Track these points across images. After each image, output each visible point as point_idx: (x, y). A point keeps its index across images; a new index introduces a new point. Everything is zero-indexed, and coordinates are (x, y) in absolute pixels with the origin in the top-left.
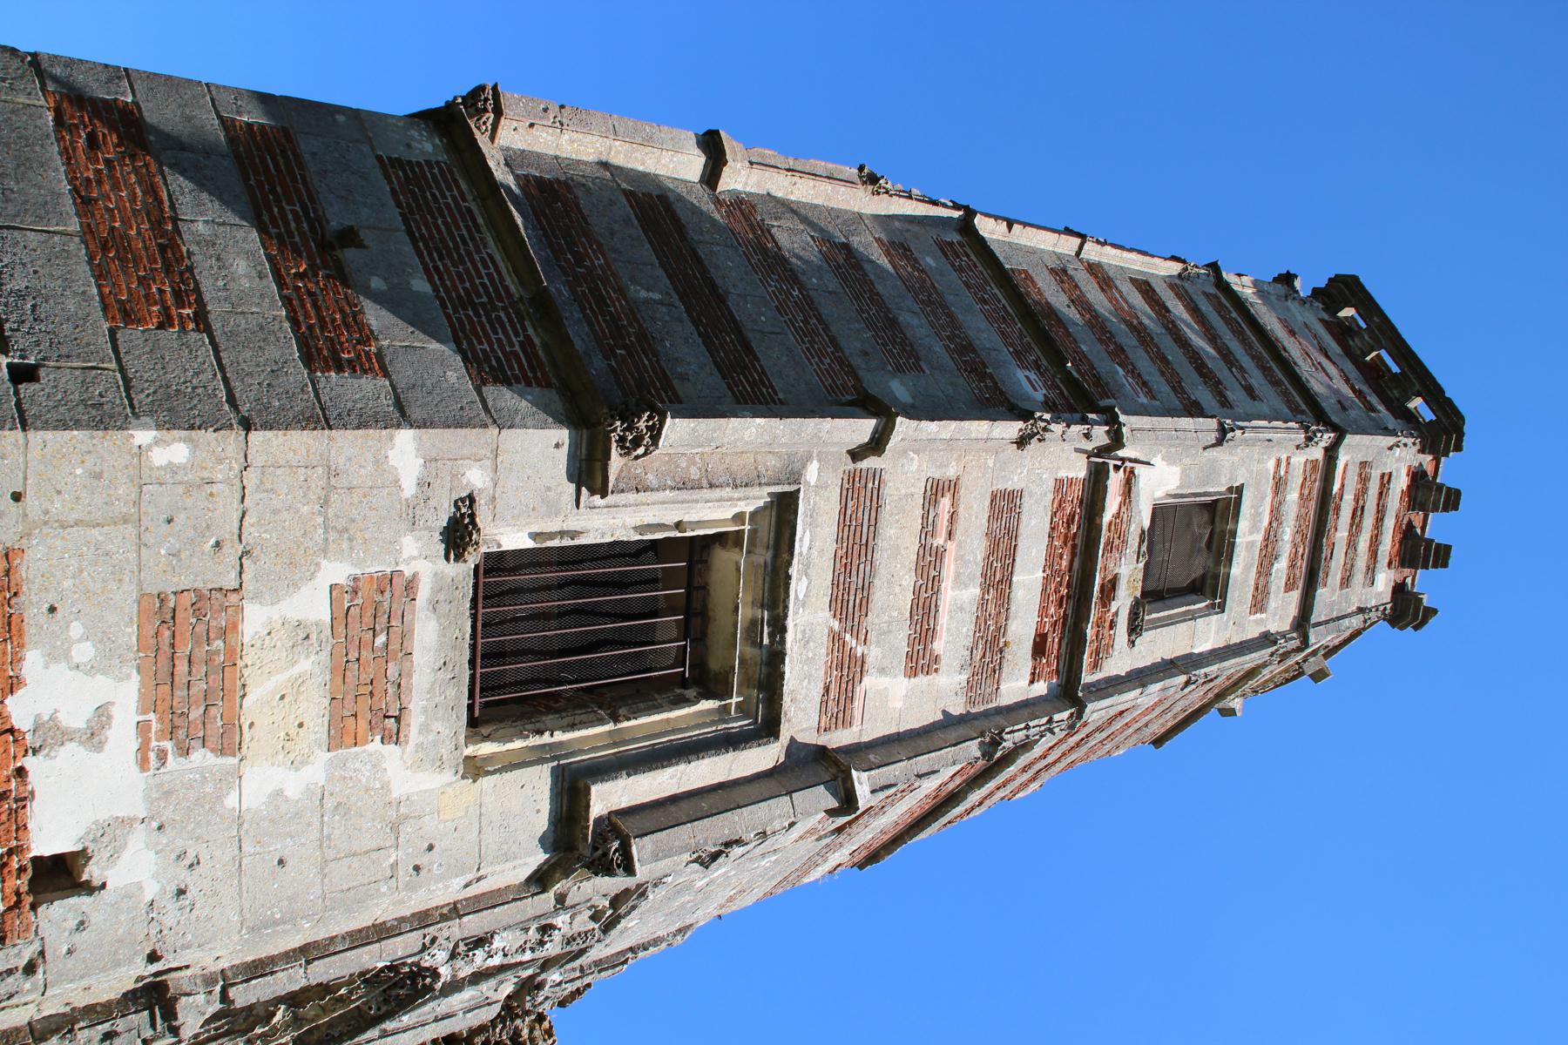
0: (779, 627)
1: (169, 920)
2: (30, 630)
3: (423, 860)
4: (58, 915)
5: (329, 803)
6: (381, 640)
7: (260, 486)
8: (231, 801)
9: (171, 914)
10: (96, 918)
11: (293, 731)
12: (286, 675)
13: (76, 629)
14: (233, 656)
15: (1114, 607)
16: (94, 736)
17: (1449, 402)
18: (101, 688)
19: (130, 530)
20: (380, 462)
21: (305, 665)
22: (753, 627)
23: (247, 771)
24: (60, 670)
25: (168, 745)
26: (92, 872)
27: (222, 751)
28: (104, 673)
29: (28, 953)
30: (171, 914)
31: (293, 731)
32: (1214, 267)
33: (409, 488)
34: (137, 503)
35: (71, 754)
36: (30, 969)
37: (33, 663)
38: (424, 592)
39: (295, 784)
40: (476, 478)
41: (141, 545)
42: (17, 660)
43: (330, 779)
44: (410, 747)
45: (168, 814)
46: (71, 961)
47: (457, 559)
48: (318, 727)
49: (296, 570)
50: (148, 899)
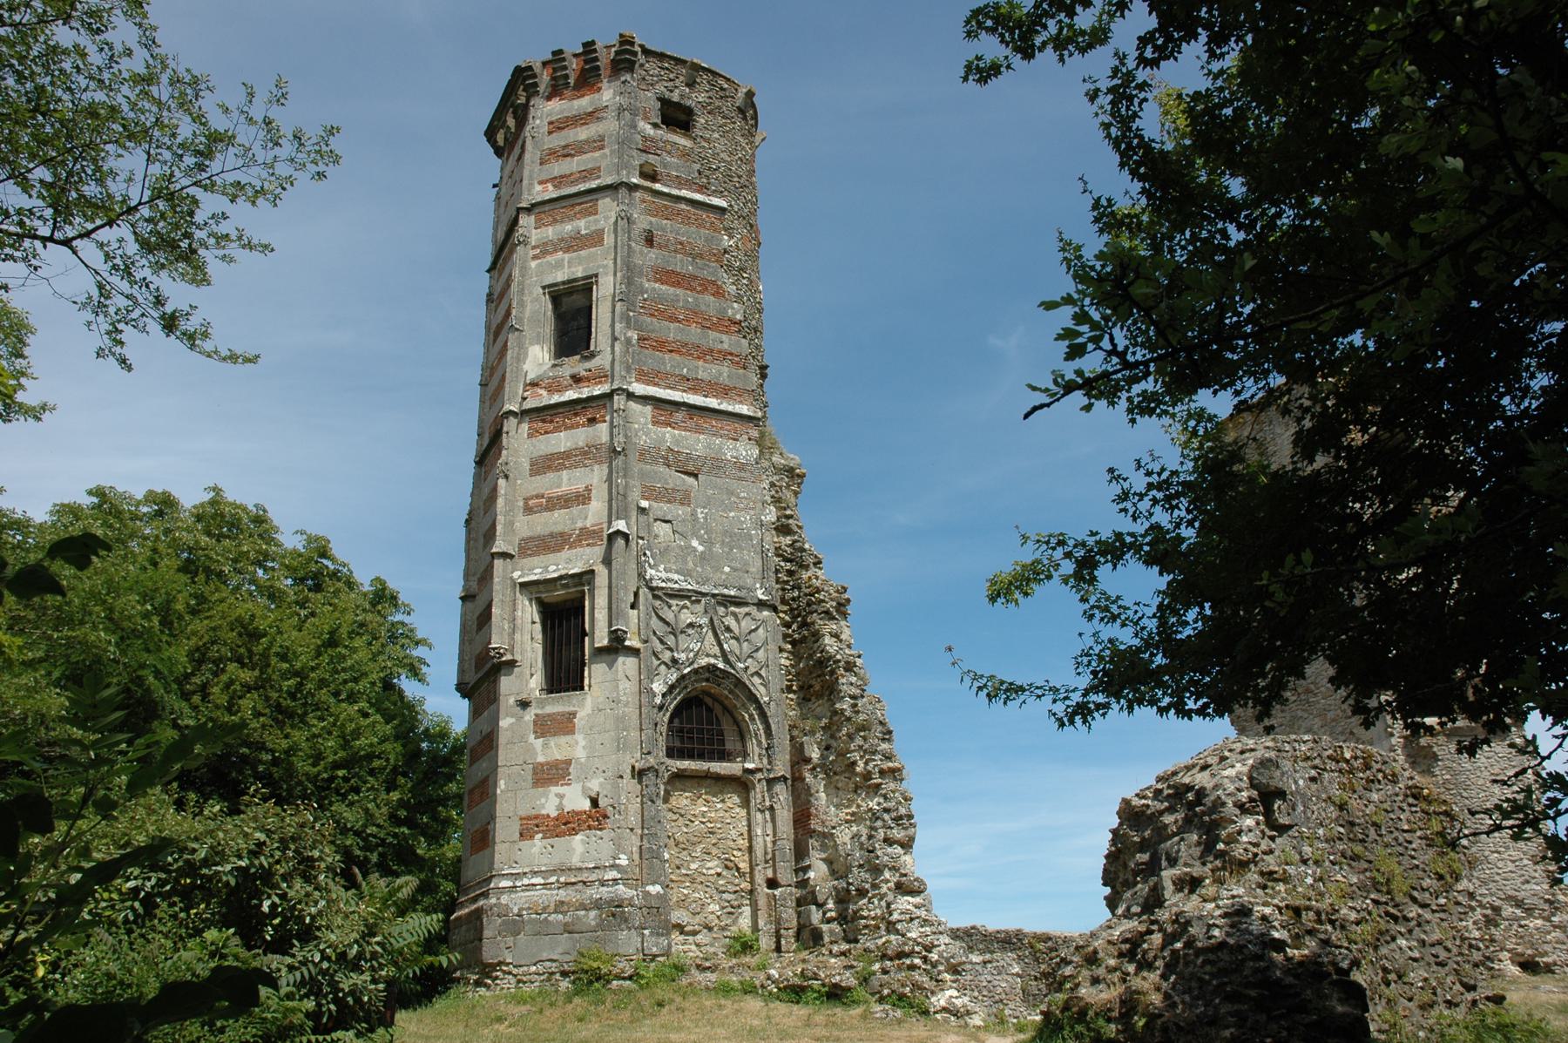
0: (561, 578)
4: (601, 803)
14: (548, 763)
15: (584, 373)
16: (561, 796)
17: (513, 75)
18: (551, 796)
21: (552, 744)
22: (565, 586)
26: (593, 795)
32: (488, 271)
33: (513, 720)
37: (544, 812)
38: (539, 712)
39: (582, 743)
40: (512, 700)
48: (568, 738)
49: (530, 750)
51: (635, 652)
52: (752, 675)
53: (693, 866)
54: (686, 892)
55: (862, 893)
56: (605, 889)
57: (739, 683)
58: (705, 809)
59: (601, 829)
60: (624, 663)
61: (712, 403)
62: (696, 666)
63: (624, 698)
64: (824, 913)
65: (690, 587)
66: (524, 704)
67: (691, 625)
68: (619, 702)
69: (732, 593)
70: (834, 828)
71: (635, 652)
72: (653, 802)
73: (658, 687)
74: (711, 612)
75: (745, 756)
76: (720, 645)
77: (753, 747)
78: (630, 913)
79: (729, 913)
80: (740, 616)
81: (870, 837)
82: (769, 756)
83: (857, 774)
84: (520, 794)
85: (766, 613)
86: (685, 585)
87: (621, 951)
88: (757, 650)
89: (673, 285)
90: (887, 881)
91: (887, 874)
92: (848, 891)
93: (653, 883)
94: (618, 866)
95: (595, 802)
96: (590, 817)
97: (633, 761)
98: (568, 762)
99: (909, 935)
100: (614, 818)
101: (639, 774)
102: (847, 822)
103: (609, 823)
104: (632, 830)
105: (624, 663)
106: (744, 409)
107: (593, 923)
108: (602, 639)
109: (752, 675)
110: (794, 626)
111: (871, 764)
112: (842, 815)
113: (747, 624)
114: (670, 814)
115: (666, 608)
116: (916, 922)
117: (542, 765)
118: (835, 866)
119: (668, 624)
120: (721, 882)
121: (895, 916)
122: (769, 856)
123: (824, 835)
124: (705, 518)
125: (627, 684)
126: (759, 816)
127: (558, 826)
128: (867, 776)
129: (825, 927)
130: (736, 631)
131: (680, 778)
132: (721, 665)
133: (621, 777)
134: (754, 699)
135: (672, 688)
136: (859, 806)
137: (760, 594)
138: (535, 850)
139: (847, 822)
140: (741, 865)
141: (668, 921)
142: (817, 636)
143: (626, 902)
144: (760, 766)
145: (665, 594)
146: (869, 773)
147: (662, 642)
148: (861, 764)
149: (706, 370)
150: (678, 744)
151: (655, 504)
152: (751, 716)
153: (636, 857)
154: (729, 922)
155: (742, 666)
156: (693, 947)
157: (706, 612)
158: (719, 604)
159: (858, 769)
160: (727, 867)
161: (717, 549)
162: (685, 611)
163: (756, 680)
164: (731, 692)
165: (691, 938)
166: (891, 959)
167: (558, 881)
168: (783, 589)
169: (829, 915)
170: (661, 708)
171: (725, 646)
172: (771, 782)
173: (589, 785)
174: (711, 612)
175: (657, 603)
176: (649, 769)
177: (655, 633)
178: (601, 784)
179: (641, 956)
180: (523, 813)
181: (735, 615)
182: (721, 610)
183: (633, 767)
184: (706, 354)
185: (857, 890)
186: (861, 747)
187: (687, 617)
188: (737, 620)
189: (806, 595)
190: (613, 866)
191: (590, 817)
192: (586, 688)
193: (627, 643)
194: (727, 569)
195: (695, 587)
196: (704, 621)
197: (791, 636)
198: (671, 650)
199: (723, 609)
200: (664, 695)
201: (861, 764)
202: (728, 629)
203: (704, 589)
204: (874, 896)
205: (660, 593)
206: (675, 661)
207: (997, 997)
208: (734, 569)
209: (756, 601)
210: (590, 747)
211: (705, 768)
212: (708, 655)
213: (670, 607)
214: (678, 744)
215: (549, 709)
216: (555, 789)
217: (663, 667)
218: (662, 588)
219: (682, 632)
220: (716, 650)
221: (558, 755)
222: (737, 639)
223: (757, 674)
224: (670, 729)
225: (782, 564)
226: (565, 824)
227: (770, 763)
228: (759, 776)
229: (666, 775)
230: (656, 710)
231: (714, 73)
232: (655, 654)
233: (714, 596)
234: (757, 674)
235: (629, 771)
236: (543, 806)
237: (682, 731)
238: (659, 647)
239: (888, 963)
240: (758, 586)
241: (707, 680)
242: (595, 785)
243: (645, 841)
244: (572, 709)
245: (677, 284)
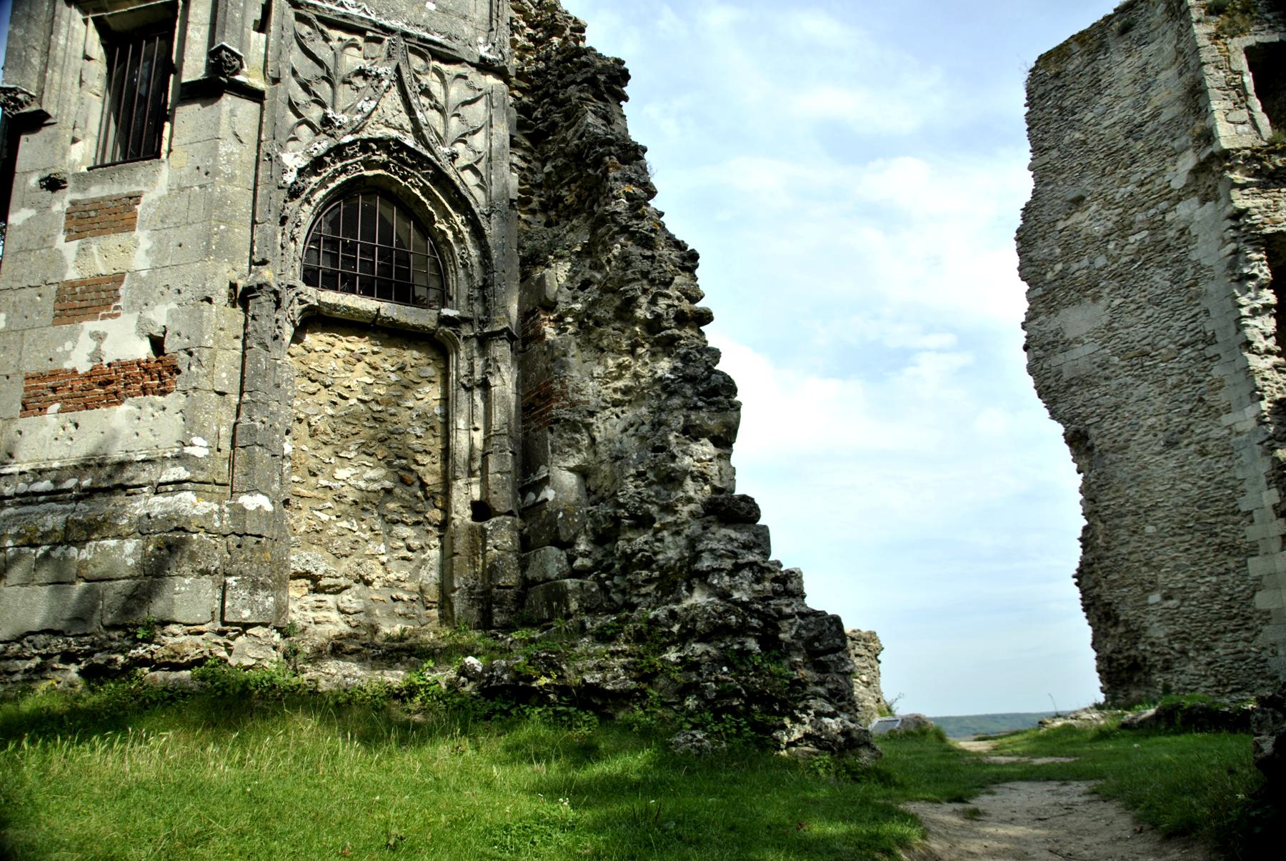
1: (189, 295)
2: (57, 367)
3: (203, 170)
4: (169, 347)
5: (159, 226)
6: (93, 214)
7: (20, 281)
8: (144, 274)
9: (187, 295)
10: (177, 328)
11: (121, 249)
12: (97, 256)
13: (60, 349)
14: (83, 282)
16: (99, 337)
19: (26, 333)
20: (20, 228)
21: (94, 248)
23: (132, 269)
24: (73, 355)
25: (114, 305)
26: (157, 332)
27: (122, 281)
28: (78, 336)
29: (183, 355)
30: (187, 295)
31: (121, 249)
34: (16, 331)
35: (105, 347)
36: (191, 354)
37: (68, 365)
38: (78, 196)
40: (33, 181)
41: (33, 328)
42: (66, 371)
43: (147, 228)
44: (145, 189)
45: (141, 302)
46: (193, 337)
47: (65, 182)
48: (123, 238)
49: (57, 260)
50: (176, 306)
51: (255, 95)
52: (464, 169)
54: (324, 517)
55: (643, 522)
56: (160, 499)
57: (441, 179)
58: (370, 381)
59: (163, 393)
60: (232, 113)
62: (365, 135)
63: (227, 169)
64: (571, 560)
65: (363, 15)
66: (53, 184)
67: (361, 73)
68: (218, 173)
69: (437, 38)
70: (592, 414)
71: (255, 95)
72: (266, 347)
73: (294, 159)
74: (398, 58)
75: (444, 300)
76: (410, 111)
77: (459, 285)
79: (404, 558)
80: (447, 77)
81: (657, 425)
82: (484, 300)
83: (636, 321)
84: (31, 336)
85: (491, 81)
86: (354, 12)
87: (178, 617)
88: (475, 132)
90: (690, 500)
91: (690, 486)
92: (616, 520)
93: (252, 491)
94: (188, 457)
95: (157, 344)
96: (146, 370)
97: (234, 276)
98: (118, 278)
99: (736, 595)
100: (192, 372)
101: (242, 297)
102: (616, 404)
103: (180, 382)
104: (222, 394)
105: (232, 113)
107: (130, 562)
108: (194, 67)
109: (464, 169)
110: (538, 114)
111: (663, 303)
112: (608, 393)
113: (457, 92)
114: (306, 382)
115: (320, 41)
116: (747, 573)
117: (73, 285)
118: (592, 483)
119: (320, 63)
120: (392, 506)
121: (706, 563)
122: (477, 465)
123: (574, 427)
125: (235, 148)
126: (463, 394)
127: (89, 389)
128: (653, 325)
129: (570, 583)
130: (441, 99)
132: (410, 141)
133: (209, 300)
134: (462, 203)
135: (317, 164)
136: (636, 376)
137: (482, 51)
138: (47, 432)
139: (616, 404)
140: (429, 479)
141: (284, 564)
142: (572, 115)
143: (195, 522)
144: (469, 315)
145: (321, 19)
146: (658, 317)
147: (305, 87)
148: (643, 300)
150: (324, 265)
152: (457, 234)
153: (226, 445)
154: (403, 574)
155: (447, 150)
156: (335, 616)
157: (389, 56)
158: (413, 50)
159: (641, 313)
160: (402, 481)
162: (354, 51)
163: (469, 177)
164: (426, 191)
165: (330, 599)
166: (704, 639)
167: (78, 485)
168: (521, 58)
169: (579, 562)
170: (294, 193)
171: (419, 115)
172: (484, 342)
173: (149, 315)
174: (398, 58)
175: (305, 30)
176: (260, 286)
177: (294, 73)
178: (171, 314)
179: (219, 626)
180: (31, 369)
181: (436, 71)
182: (417, 62)
183: (233, 286)
185: (632, 516)
186: (645, 275)
187: (353, 60)
188: (444, 82)
189: (558, 63)
190: (180, 458)
191: (146, 370)
192: (164, 156)
193: (239, 78)
194: (431, 6)
195: (373, 17)
196: (385, 69)
197: (531, 127)
198: (323, 105)
200: (301, 172)
201: (643, 300)
202: (426, 92)
203: (387, 23)
204: (664, 527)
205: (310, 14)
206: (327, 121)
209: (476, 60)
210: (158, 251)
212: (388, 124)
213: (327, 40)
214: (324, 265)
215: (96, 192)
216: (90, 326)
217: (304, 129)
219: (344, 82)
220: (404, 119)
221: (100, 266)
222: (441, 111)
223: (471, 167)
224: (314, 239)
225: (523, 23)
226: (102, 385)
227: (487, 311)
228: (466, 331)
229: (298, 308)
230: (284, 194)
232: (293, 107)
233: (405, 35)
234: (471, 167)
235: (224, 291)
236: (67, 355)
237: (333, 243)
238: (301, 96)
239: (699, 648)
240: (481, 40)
241: (385, 166)
242: (160, 316)
243: (243, 413)
244: (134, 189)
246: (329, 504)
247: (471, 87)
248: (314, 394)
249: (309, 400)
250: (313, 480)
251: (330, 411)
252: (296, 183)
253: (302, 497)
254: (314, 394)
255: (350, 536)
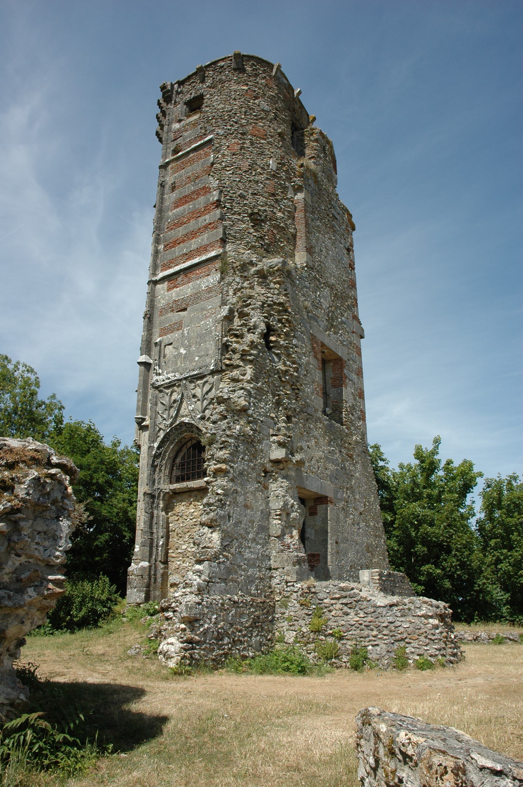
53: (184, 547)
54: (179, 563)
61: (196, 260)
69: (195, 373)
78: (132, 579)
86: (173, 378)
89: (183, 204)
106: (213, 254)
124: (188, 333)
131: (176, 494)
145: (165, 388)
149: (194, 243)
151: (165, 337)
161: (193, 348)
184: (194, 234)
194: (197, 358)
199: (193, 384)
200: (159, 448)
207: (399, 636)
208: (201, 357)
209: (209, 372)
211: (185, 486)
218: (162, 385)
229: (162, 495)
231: (215, 63)
233: (186, 379)
245: (186, 202)
246: (180, 558)
247: (210, 384)
248: (177, 520)
249: (176, 522)
250: (177, 551)
251: (181, 525)
252: (156, 452)
253: (173, 557)
254: (177, 520)
255: (186, 569)
